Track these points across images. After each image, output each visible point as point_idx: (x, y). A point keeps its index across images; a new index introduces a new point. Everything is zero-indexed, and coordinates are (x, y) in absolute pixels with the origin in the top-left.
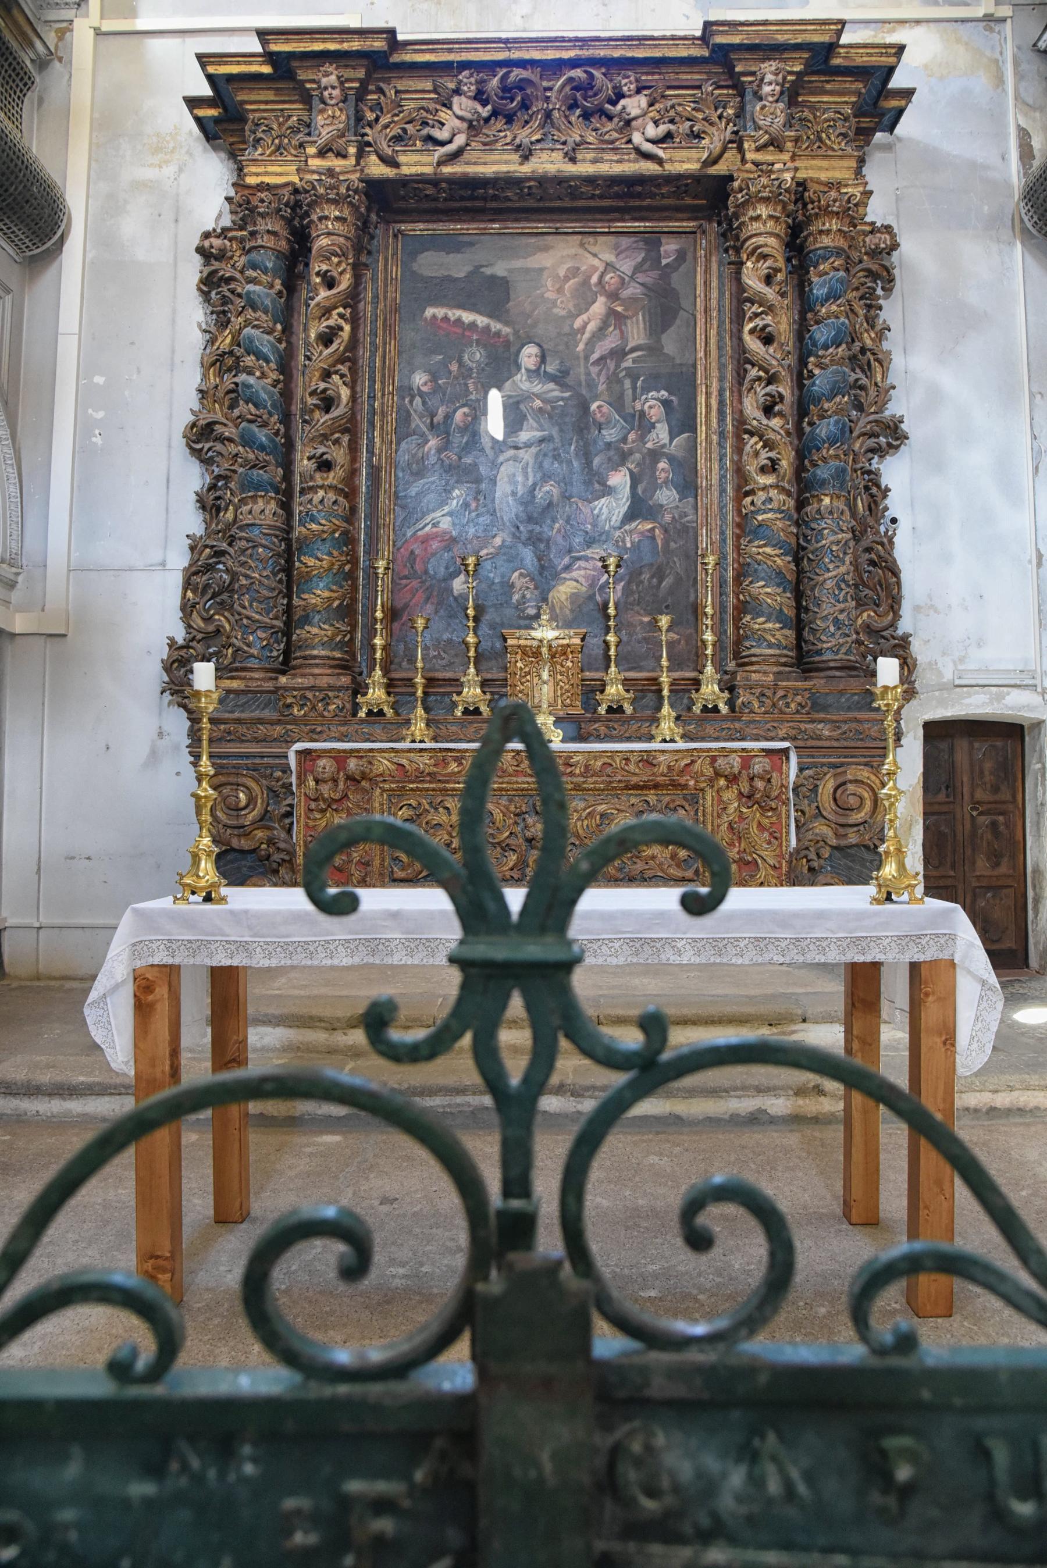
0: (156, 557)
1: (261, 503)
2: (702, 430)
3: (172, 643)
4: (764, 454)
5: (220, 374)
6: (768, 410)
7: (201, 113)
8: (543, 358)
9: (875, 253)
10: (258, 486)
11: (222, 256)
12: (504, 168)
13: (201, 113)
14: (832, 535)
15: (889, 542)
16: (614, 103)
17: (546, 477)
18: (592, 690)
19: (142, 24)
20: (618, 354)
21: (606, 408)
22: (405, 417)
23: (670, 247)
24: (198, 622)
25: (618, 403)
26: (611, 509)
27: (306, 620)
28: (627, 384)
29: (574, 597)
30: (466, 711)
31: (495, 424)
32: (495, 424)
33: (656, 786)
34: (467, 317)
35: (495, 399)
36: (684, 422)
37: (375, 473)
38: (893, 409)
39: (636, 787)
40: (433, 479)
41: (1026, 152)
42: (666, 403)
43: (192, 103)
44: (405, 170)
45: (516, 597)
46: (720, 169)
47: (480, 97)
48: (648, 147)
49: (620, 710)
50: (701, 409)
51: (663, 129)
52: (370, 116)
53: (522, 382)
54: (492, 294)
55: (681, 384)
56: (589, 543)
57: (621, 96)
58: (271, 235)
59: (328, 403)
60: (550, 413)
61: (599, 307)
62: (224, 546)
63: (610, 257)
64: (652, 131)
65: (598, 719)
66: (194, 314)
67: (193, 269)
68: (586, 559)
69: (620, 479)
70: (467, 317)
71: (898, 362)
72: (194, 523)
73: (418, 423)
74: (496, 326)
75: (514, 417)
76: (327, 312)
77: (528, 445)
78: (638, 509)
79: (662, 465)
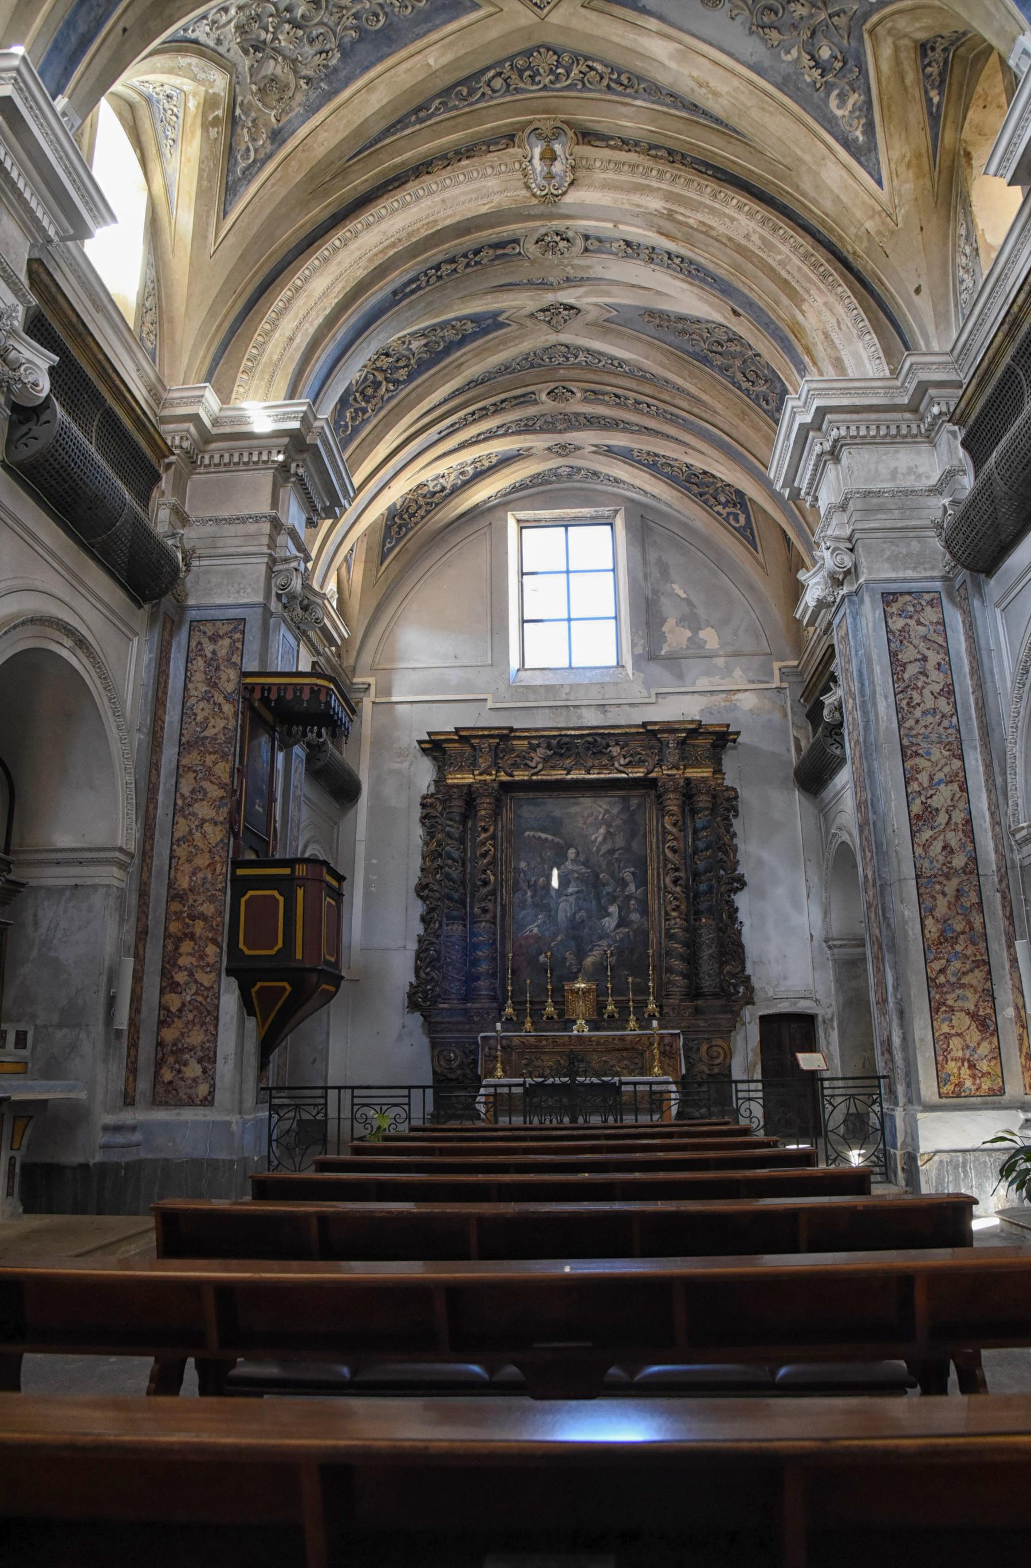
0: (401, 943)
1: (456, 926)
2: (650, 886)
3: (411, 983)
4: (675, 903)
5: (432, 861)
6: (675, 882)
7: (423, 746)
8: (578, 854)
9: (728, 800)
10: (454, 918)
11: (432, 805)
12: (559, 777)
13: (423, 746)
14: (707, 936)
15: (740, 932)
16: (606, 749)
17: (580, 909)
18: (601, 1007)
19: (394, 699)
20: (611, 852)
21: (607, 876)
22: (516, 882)
23: (634, 801)
24: (423, 975)
25: (612, 875)
26: (610, 923)
27: (478, 979)
28: (616, 865)
29: (594, 963)
30: (548, 1018)
31: (555, 883)
32: (555, 883)
33: (626, 1049)
34: (543, 836)
35: (555, 872)
36: (642, 882)
37: (503, 907)
38: (741, 870)
39: (618, 1050)
40: (529, 910)
41: (798, 749)
42: (633, 873)
43: (420, 742)
44: (516, 778)
45: (568, 964)
46: (653, 775)
47: (549, 747)
48: (621, 768)
49: (613, 1016)
50: (649, 877)
51: (627, 760)
52: (501, 755)
53: (569, 865)
54: (554, 826)
55: (641, 864)
56: (601, 938)
57: (608, 746)
58: (457, 805)
59: (485, 883)
60: (581, 879)
61: (602, 830)
62: (434, 940)
63: (605, 807)
64: (622, 762)
65: (603, 1020)
66: (418, 831)
67: (417, 812)
68: (599, 946)
69: (613, 909)
70: (543, 836)
71: (741, 847)
72: (419, 929)
73: (524, 886)
74: (557, 840)
75: (564, 880)
76: (484, 844)
77: (572, 894)
78: (622, 922)
79: (632, 902)
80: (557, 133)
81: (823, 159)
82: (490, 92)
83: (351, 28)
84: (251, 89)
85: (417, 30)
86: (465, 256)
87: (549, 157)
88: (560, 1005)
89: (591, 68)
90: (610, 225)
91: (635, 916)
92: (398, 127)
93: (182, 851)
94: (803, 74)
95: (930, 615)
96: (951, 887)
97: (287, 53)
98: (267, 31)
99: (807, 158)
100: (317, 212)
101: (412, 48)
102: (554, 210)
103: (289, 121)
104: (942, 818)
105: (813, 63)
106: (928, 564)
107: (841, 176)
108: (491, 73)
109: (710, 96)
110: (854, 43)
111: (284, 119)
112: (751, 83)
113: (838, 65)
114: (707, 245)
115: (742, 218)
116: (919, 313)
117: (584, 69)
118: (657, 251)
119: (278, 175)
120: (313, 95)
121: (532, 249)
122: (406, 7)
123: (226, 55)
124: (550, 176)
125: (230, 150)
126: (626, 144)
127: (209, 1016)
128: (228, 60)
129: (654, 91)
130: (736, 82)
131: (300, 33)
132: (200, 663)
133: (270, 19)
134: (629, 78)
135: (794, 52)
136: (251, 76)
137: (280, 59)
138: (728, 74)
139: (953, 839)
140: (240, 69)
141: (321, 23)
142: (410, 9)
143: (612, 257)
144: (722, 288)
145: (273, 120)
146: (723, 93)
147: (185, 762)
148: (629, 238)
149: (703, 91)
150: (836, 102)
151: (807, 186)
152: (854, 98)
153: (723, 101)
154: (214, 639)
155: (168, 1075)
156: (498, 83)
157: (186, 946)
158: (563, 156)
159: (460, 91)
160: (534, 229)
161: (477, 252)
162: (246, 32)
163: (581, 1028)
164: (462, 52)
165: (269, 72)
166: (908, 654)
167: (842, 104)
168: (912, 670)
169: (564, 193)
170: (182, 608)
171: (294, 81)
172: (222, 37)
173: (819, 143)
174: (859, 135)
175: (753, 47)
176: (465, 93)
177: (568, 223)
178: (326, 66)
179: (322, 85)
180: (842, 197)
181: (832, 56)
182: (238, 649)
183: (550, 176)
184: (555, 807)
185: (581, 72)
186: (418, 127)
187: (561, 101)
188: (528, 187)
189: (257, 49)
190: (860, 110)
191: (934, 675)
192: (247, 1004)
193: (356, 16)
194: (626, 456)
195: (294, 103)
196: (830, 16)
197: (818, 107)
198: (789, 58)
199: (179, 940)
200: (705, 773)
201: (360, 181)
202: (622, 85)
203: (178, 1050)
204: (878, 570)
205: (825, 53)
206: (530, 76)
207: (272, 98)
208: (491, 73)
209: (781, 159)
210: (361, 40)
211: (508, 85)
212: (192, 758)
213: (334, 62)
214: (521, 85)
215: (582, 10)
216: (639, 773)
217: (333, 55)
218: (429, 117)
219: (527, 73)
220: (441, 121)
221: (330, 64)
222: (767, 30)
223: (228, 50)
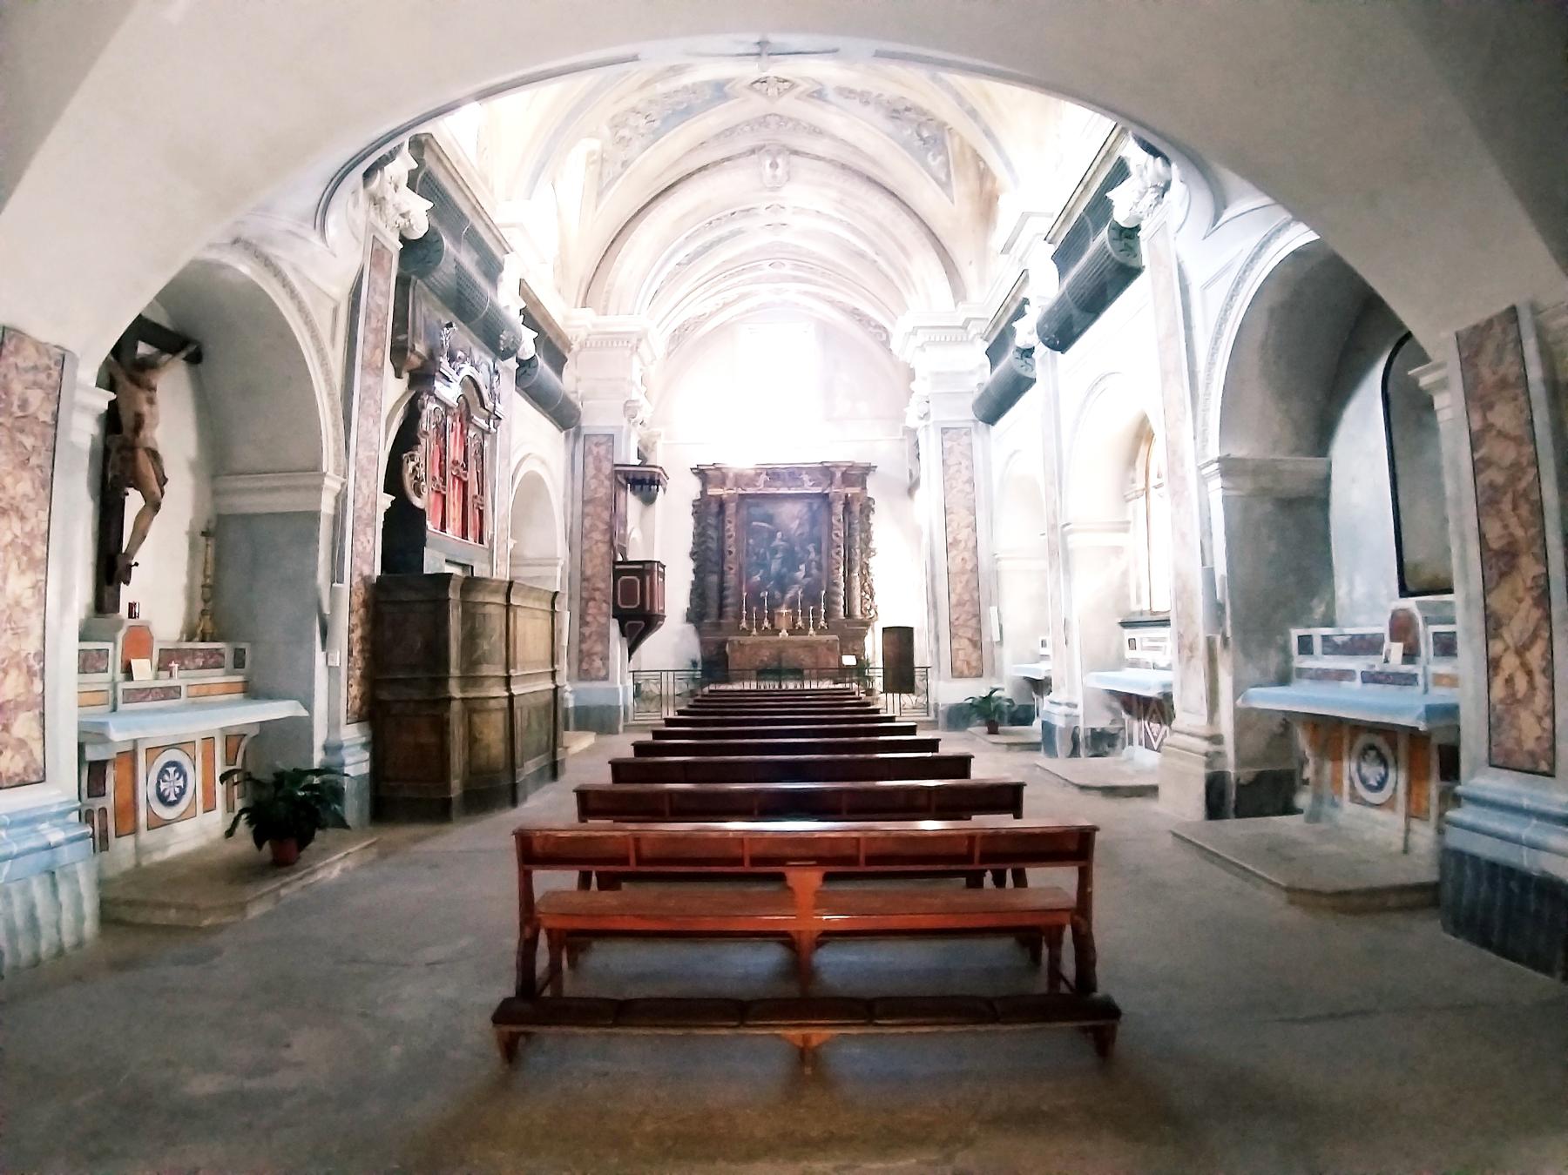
18: (794, 621)
26: (800, 574)
36: (818, 551)
54: (769, 519)
58: (714, 508)
69: (802, 567)
72: (692, 577)
80: (779, 153)
87: (774, 165)
88: (771, 620)
91: (814, 571)
93: (587, 556)
95: (965, 440)
96: (964, 578)
104: (962, 545)
106: (964, 413)
116: (969, 274)
124: (774, 177)
125: (601, 174)
126: (818, 158)
127: (604, 637)
129: (833, 137)
132: (590, 459)
139: (967, 555)
144: (871, 243)
147: (587, 510)
154: (597, 445)
155: (585, 666)
157: (591, 604)
163: (784, 633)
166: (951, 461)
168: (952, 470)
170: (579, 428)
174: (943, 177)
175: (889, 126)
182: (611, 450)
183: (774, 177)
184: (769, 508)
191: (964, 471)
192: (623, 633)
194: (816, 296)
199: (588, 601)
200: (857, 490)
203: (590, 655)
204: (942, 416)
205: (925, 134)
212: (589, 509)
216: (818, 490)
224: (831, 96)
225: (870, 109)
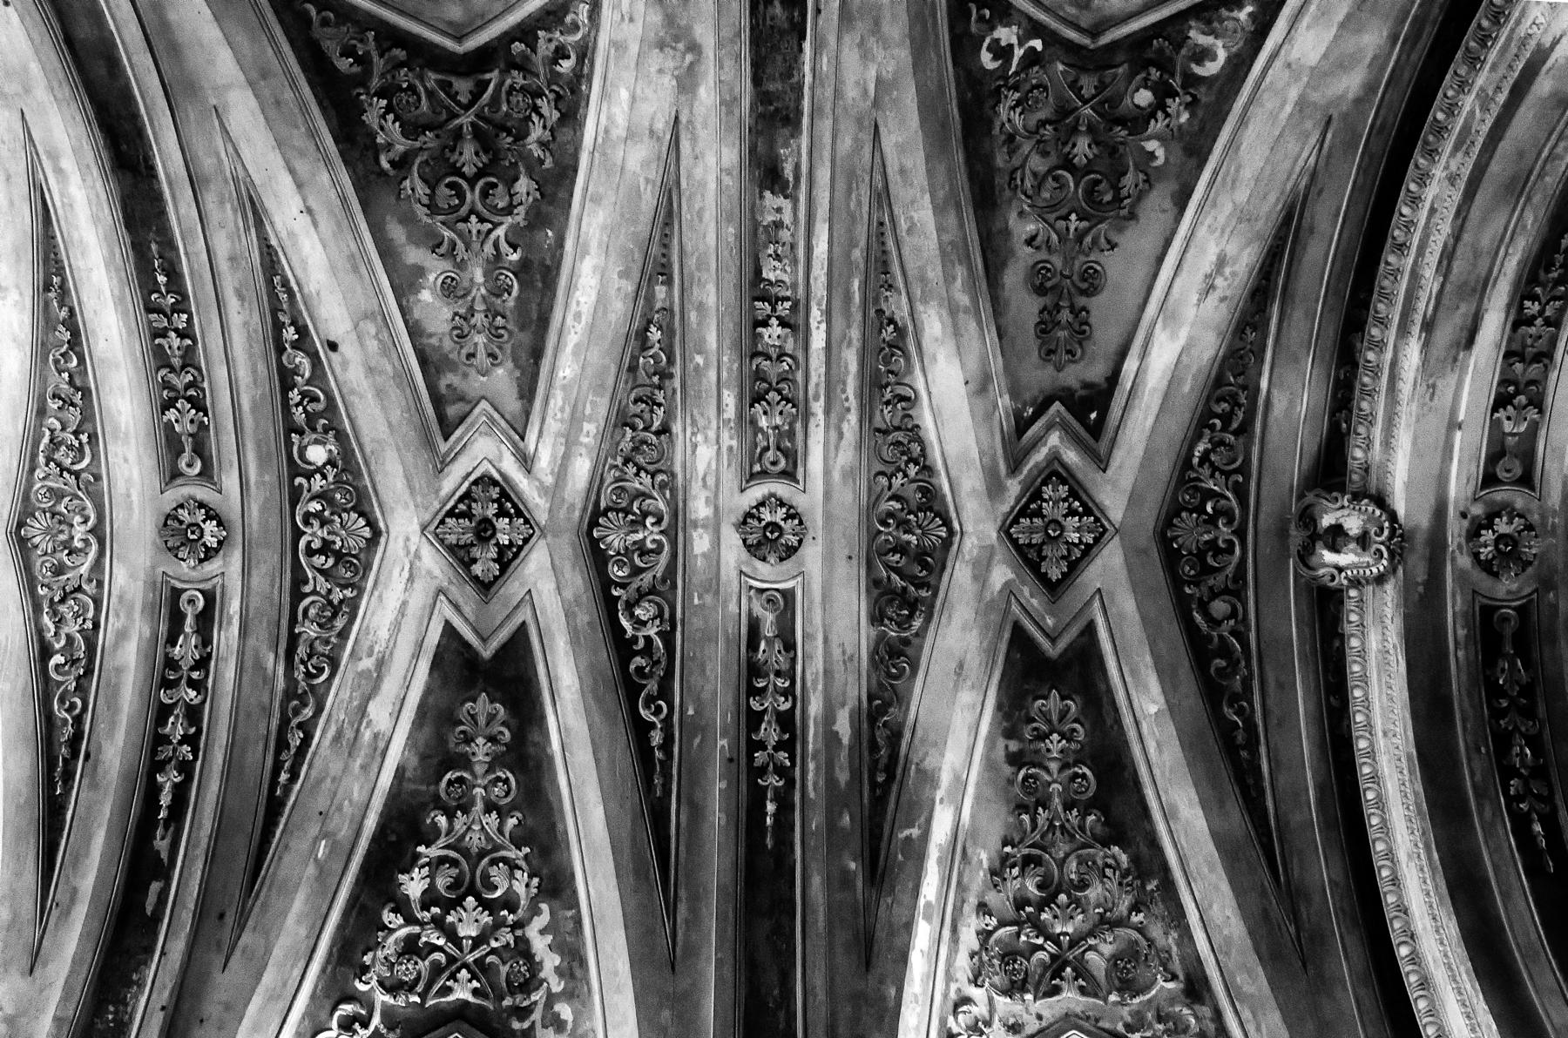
80: (1307, 518)
81: (1289, 65)
82: (1232, 622)
83: (1084, 819)
84: (1115, 1004)
85: (1109, 722)
86: (1497, 714)
87: (1336, 537)
89: (1205, 458)
90: (1458, 434)
92: (1251, 781)
94: (1180, 127)
97: (1087, 927)
98: (1041, 948)
99: (1293, 94)
100: (1345, 963)
101: (1132, 734)
102: (1420, 539)
103: (1182, 959)
105: (1160, 115)
107: (1308, 28)
108: (1198, 617)
109: (1227, 271)
110: (1120, 57)
111: (1176, 966)
112: (1201, 208)
113: (1155, 74)
114: (1477, 254)
115: (1430, 192)
117: (1206, 471)
118: (1515, 347)
119: (1246, 1014)
120: (1159, 908)
121: (1508, 587)
122: (1074, 730)
123: (1044, 1024)
124: (1363, 541)
128: (1051, 1025)
130: (1202, 231)
131: (1063, 898)
133: (1023, 938)
134: (1218, 401)
135: (1151, 146)
136: (1096, 996)
137: (1091, 941)
138: (1192, 244)
140: (1078, 1010)
141: (1062, 863)
142: (1076, 726)
143: (1543, 432)
145: (1171, 985)
146: (1217, 251)
148: (1486, 399)
149: (1219, 282)
150: (1208, 64)
151: (1351, 83)
152: (1198, 37)
153: (1231, 250)
156: (1219, 607)
158: (1339, 513)
159: (1217, 669)
160: (1461, 576)
161: (1494, 691)
162: (1025, 981)
164: (1148, 658)
165: (1103, 964)
167: (1204, 55)
169: (1393, 517)
171: (1129, 931)
172: (1012, 1021)
173: (1268, 79)
176: (1224, 663)
177: (1451, 512)
178: (1124, 875)
179: (1149, 888)
180: (1340, 17)
181: (1146, 87)
183: (1363, 541)
185: (1212, 476)
186: (1263, 750)
187: (1264, 509)
188: (1380, 580)
189: (1057, 974)
190: (1209, 22)
193: (1068, 807)
195: (1161, 941)
196: (1085, 102)
197: (1220, 92)
198: (1160, 153)
201: (1322, 870)
202: (1232, 411)
205: (1144, 97)
206: (1214, 556)
207: (1141, 974)
208: (1198, 617)
209: (1313, 140)
210: (1105, 810)
211: (1226, 591)
213: (1124, 858)
214: (1230, 570)
215: (1109, 472)
217: (1114, 857)
218: (1251, 726)
219: (1210, 560)
220: (1264, 705)
221: (1125, 865)
222: (1124, 192)
223: (1040, 1017)
224: (1096, 372)
225: (1113, 265)
